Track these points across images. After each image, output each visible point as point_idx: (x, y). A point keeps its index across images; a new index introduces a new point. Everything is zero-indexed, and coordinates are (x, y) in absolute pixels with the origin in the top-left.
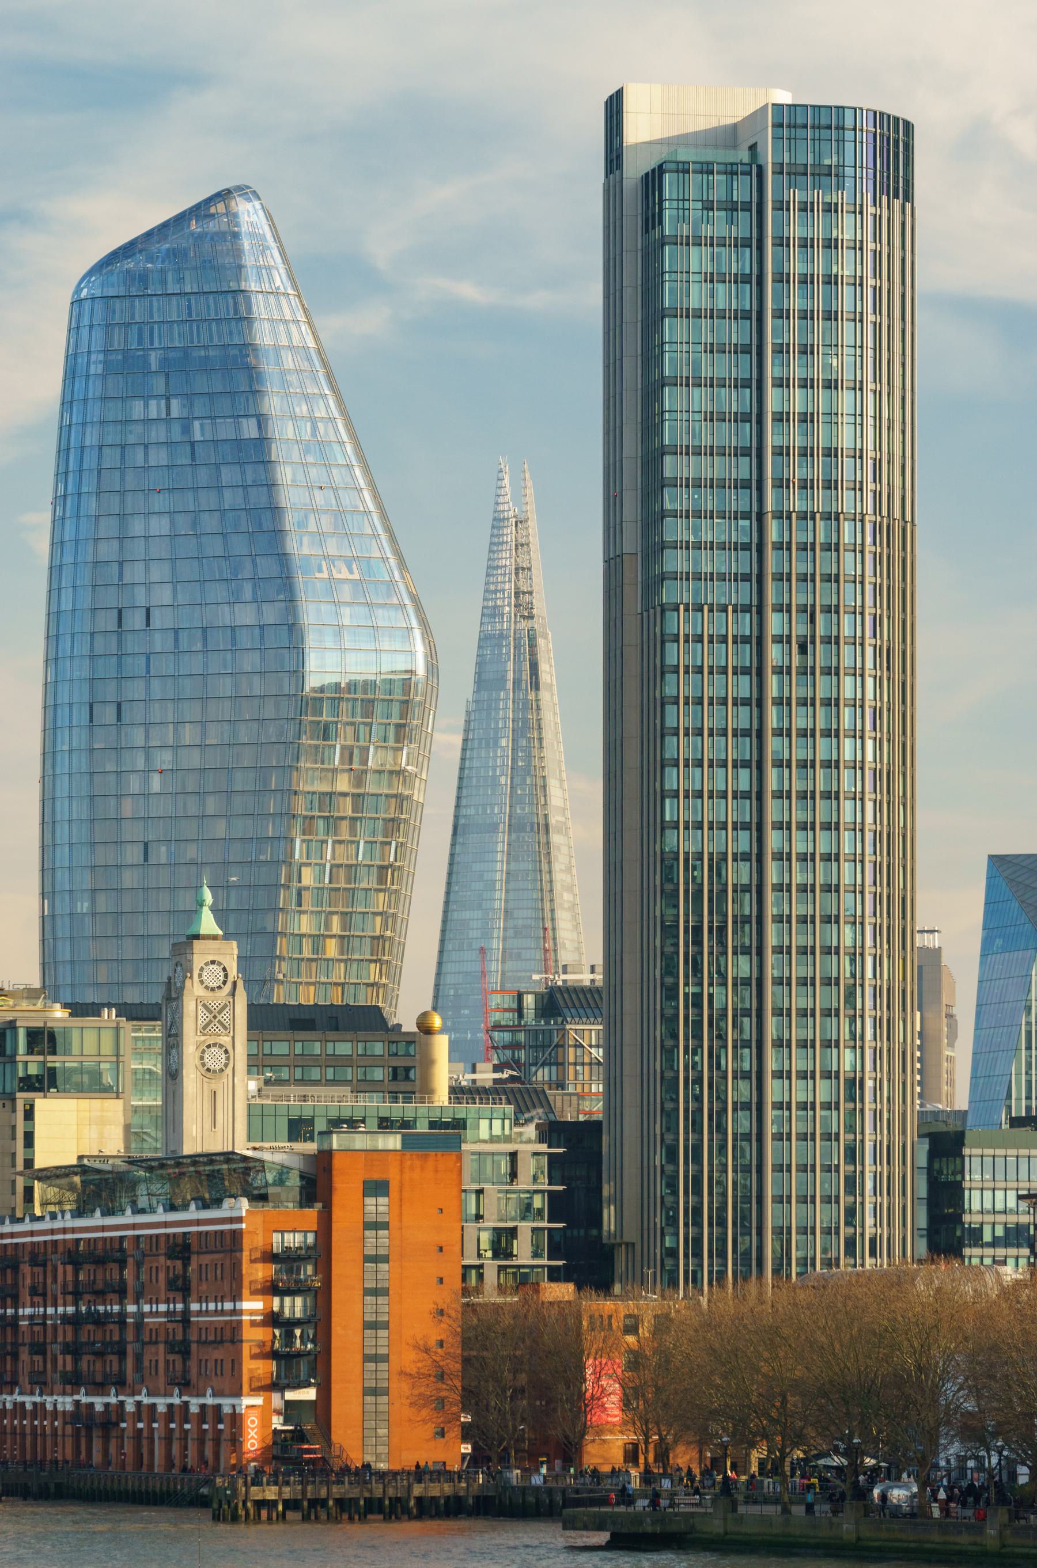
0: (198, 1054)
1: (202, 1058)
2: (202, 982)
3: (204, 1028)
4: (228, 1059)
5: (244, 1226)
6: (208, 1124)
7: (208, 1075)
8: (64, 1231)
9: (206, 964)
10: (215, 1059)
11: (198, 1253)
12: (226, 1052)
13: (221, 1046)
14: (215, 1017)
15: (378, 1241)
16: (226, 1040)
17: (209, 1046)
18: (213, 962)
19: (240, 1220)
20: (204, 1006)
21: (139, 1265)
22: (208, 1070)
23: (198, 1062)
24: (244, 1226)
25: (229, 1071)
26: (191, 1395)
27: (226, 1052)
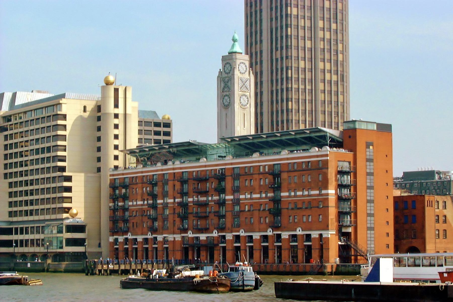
0: (239, 98)
1: (240, 100)
2: (239, 70)
3: (241, 88)
4: (248, 101)
5: (329, 158)
6: (242, 126)
7: (243, 107)
8: (174, 169)
9: (240, 63)
10: (244, 100)
11: (289, 172)
12: (248, 98)
13: (246, 96)
14: (244, 84)
15: (370, 167)
16: (248, 94)
17: (242, 96)
18: (242, 63)
19: (327, 155)
20: (241, 79)
21: (234, 179)
22: (242, 105)
23: (239, 101)
24: (329, 158)
25: (248, 105)
26: (282, 231)
27: (248, 98)
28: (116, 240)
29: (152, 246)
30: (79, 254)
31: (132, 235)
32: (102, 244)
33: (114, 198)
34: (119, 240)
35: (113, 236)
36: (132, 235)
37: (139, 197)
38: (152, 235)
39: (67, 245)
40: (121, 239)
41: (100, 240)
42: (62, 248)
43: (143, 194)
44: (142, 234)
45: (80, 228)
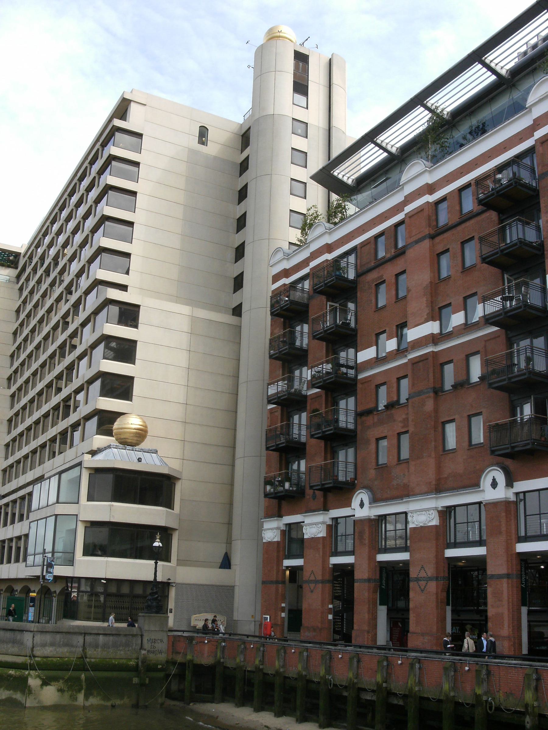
28: (293, 541)
29: (510, 547)
30: (125, 590)
31: (375, 500)
32: (236, 560)
33: (287, 358)
34: (309, 532)
35: (280, 516)
36: (375, 500)
37: (418, 304)
38: (509, 484)
39: (89, 551)
40: (314, 525)
41: (229, 542)
42: (71, 562)
43: (437, 285)
44: (439, 489)
45: (153, 487)
